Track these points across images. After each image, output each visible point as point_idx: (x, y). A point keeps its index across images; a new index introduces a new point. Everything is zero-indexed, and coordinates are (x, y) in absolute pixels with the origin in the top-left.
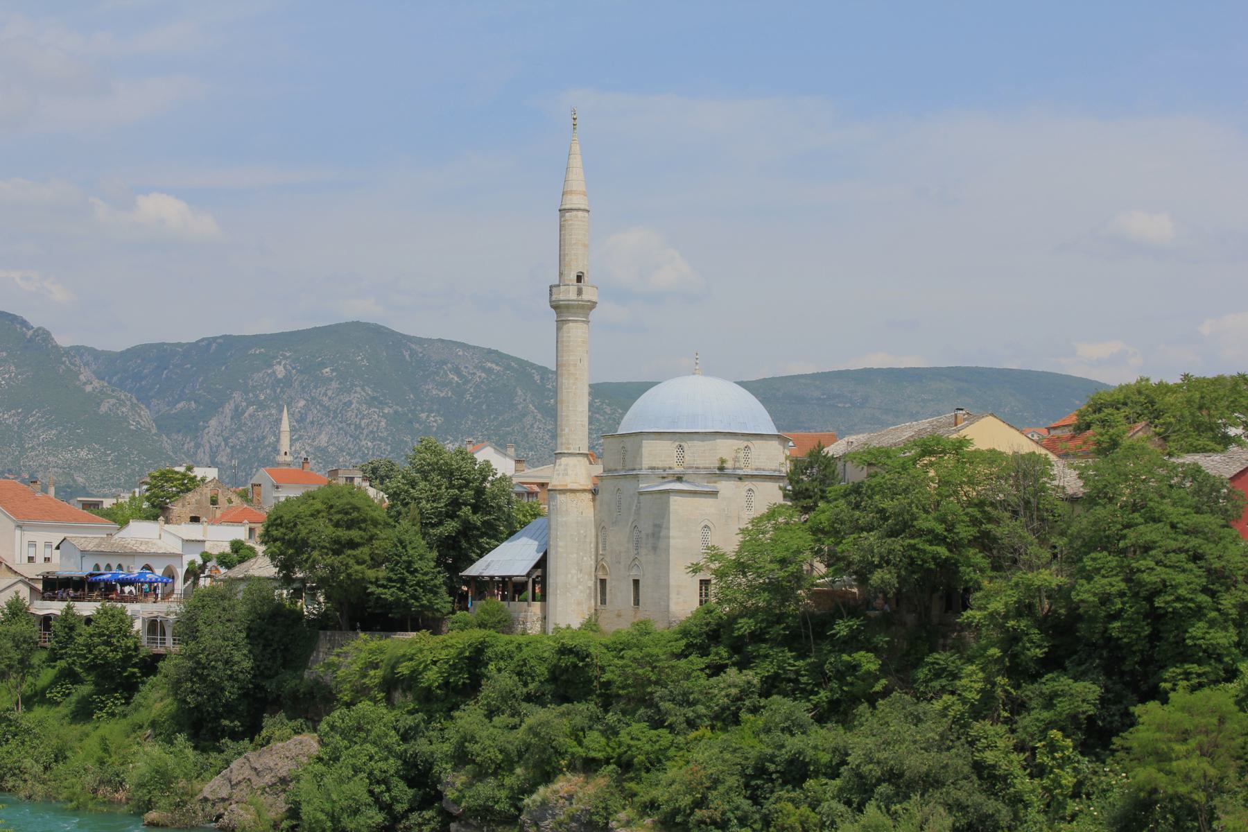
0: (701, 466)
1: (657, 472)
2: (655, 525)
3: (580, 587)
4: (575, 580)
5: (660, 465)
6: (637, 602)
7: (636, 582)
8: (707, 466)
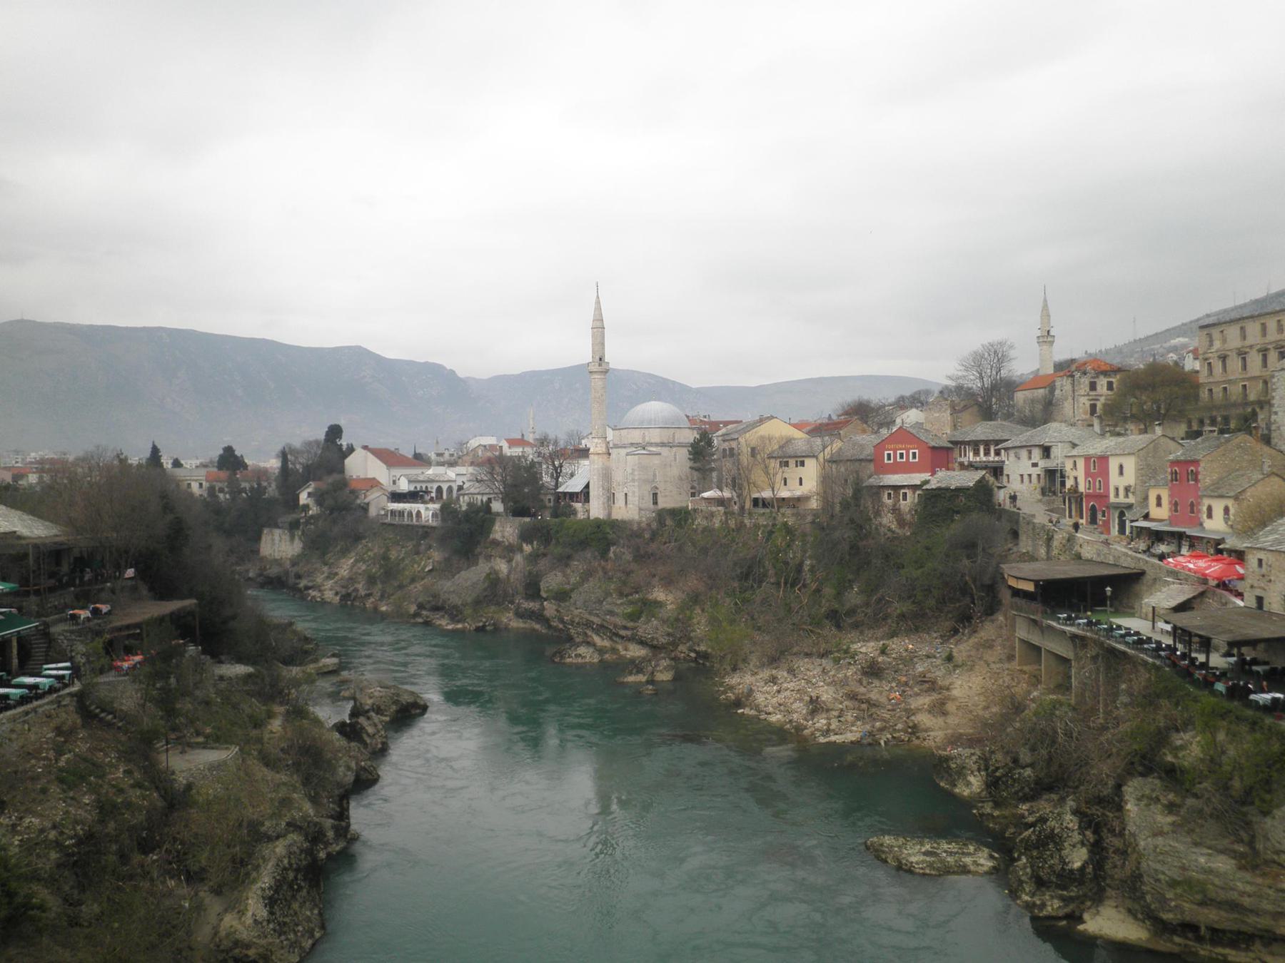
7: (626, 494)
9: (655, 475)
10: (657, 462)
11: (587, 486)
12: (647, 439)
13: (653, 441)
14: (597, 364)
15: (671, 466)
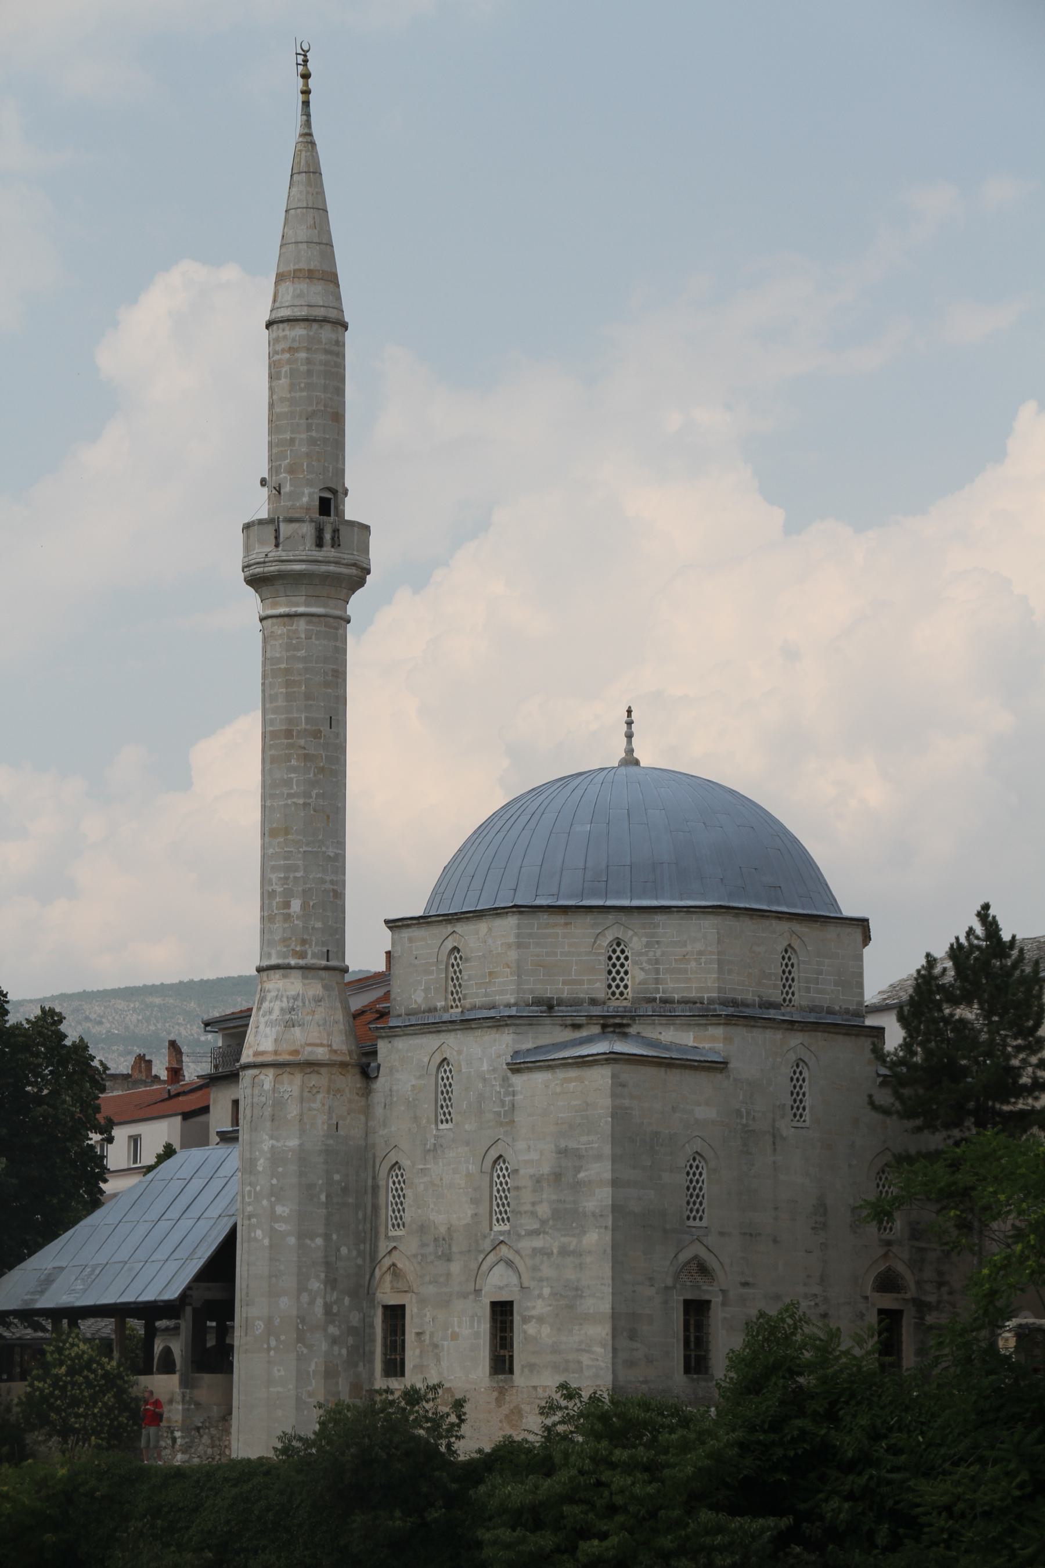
3: (332, 1330)
4: (319, 1309)
5: (566, 993)
8: (693, 994)
9: (693, 1192)
10: (705, 1113)
12: (636, 977)
13: (674, 987)
14: (307, 530)
15: (776, 1136)
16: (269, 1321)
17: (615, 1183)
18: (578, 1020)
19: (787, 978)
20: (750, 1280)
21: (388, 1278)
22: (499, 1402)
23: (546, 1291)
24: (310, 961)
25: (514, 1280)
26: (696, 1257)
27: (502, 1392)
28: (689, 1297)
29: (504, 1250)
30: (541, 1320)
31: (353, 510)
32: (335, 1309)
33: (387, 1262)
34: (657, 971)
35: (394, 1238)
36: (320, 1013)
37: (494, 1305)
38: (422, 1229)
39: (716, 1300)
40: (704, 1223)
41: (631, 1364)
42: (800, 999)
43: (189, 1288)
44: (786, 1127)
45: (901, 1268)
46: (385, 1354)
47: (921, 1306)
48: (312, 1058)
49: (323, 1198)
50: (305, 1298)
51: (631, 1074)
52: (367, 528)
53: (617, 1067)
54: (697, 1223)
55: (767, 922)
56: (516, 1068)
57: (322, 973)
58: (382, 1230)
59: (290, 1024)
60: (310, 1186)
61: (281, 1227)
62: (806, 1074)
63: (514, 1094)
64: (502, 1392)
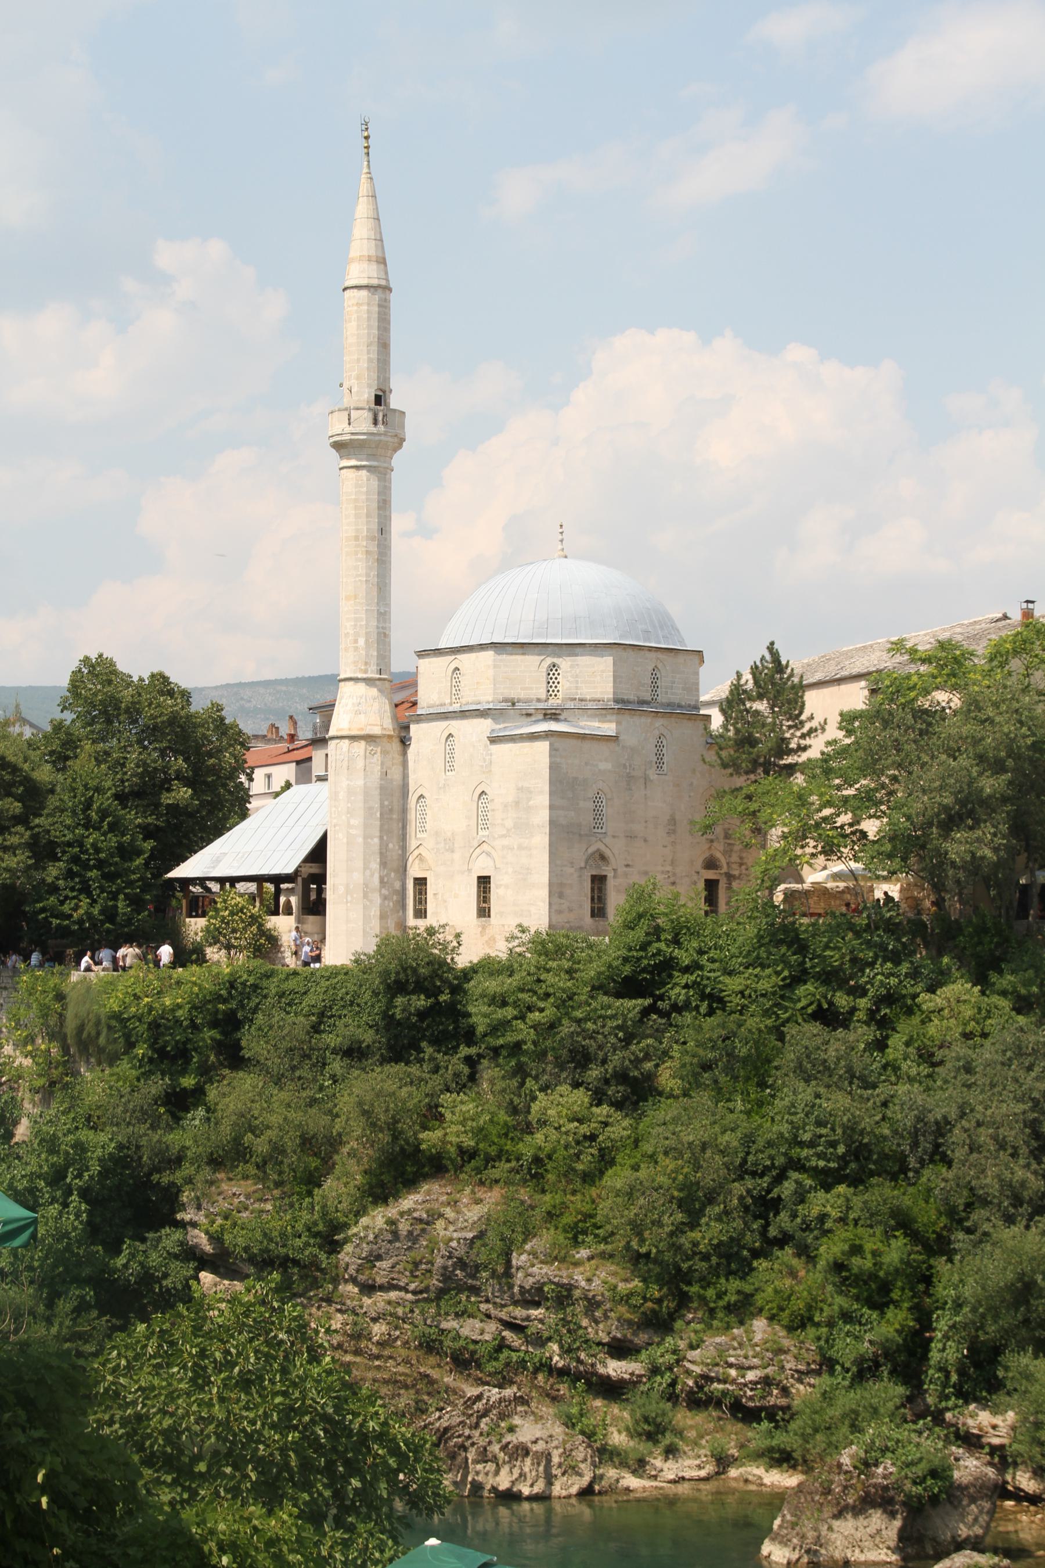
0: (588, 697)
1: (518, 706)
2: (520, 789)
5: (522, 695)
6: (484, 912)
7: (484, 882)
8: (598, 696)
9: (598, 813)
11: (318, 854)
12: (565, 686)
14: (367, 415)
15: (646, 779)
16: (347, 886)
17: (552, 807)
18: (529, 712)
19: (654, 686)
20: (630, 863)
21: (417, 861)
22: (482, 933)
23: (510, 870)
24: (369, 675)
25: (491, 864)
26: (598, 850)
27: (484, 928)
28: (594, 873)
29: (485, 846)
30: (507, 887)
31: (395, 402)
32: (386, 880)
33: (416, 853)
34: (577, 682)
35: (420, 839)
36: (376, 706)
37: (479, 878)
38: (437, 834)
39: (610, 875)
40: (603, 831)
41: (560, 912)
42: (662, 698)
43: (299, 866)
44: (652, 774)
45: (718, 855)
46: (415, 906)
47: (730, 877)
48: (371, 733)
49: (378, 815)
50: (368, 873)
51: (560, 743)
52: (404, 413)
53: (553, 739)
54: (600, 831)
55: (642, 653)
56: (494, 740)
57: (378, 682)
58: (413, 834)
59: (358, 713)
60: (370, 808)
61: (353, 832)
62: (664, 743)
63: (491, 755)
64: (484, 928)
